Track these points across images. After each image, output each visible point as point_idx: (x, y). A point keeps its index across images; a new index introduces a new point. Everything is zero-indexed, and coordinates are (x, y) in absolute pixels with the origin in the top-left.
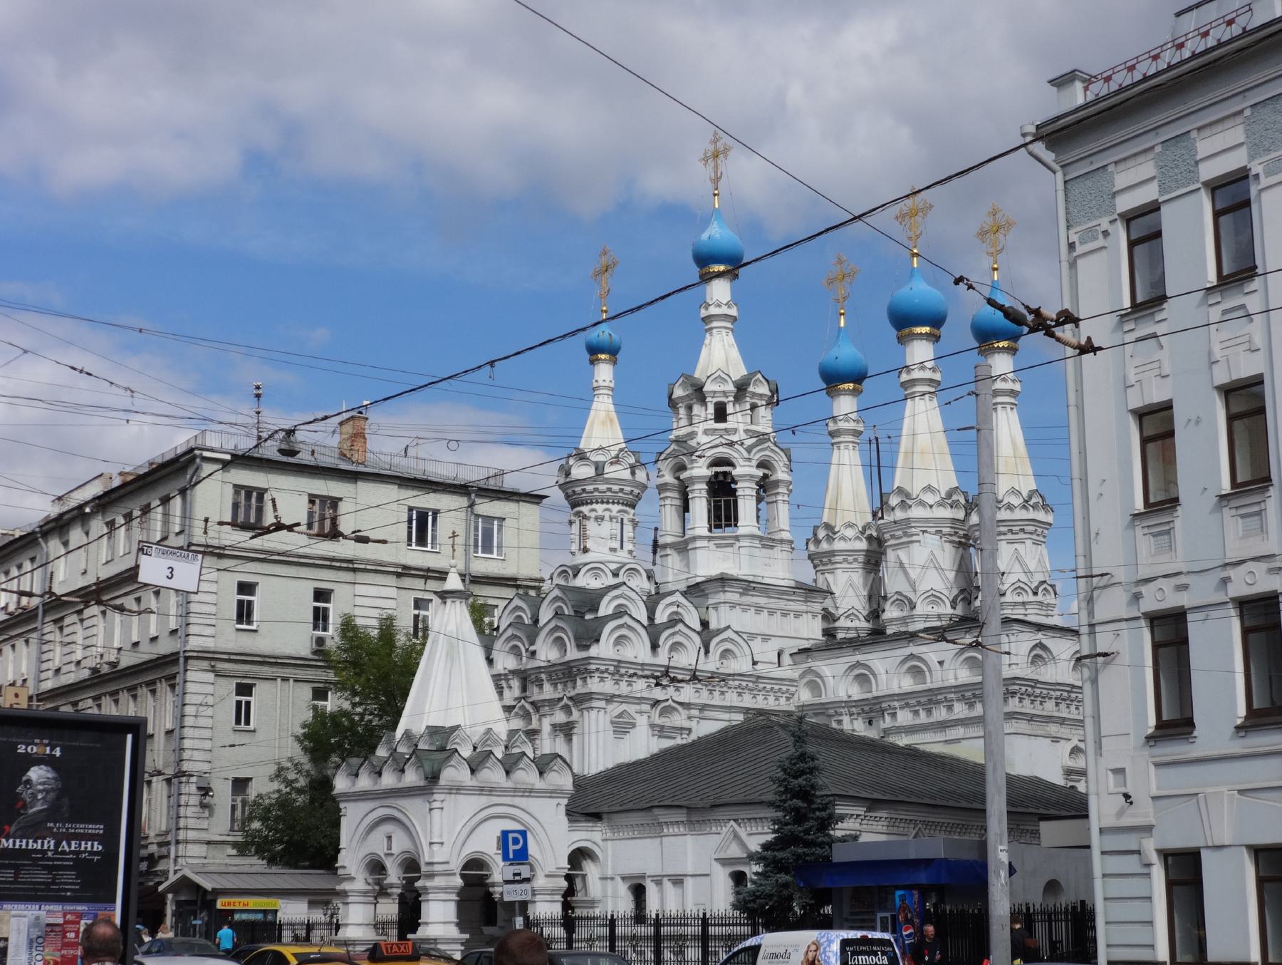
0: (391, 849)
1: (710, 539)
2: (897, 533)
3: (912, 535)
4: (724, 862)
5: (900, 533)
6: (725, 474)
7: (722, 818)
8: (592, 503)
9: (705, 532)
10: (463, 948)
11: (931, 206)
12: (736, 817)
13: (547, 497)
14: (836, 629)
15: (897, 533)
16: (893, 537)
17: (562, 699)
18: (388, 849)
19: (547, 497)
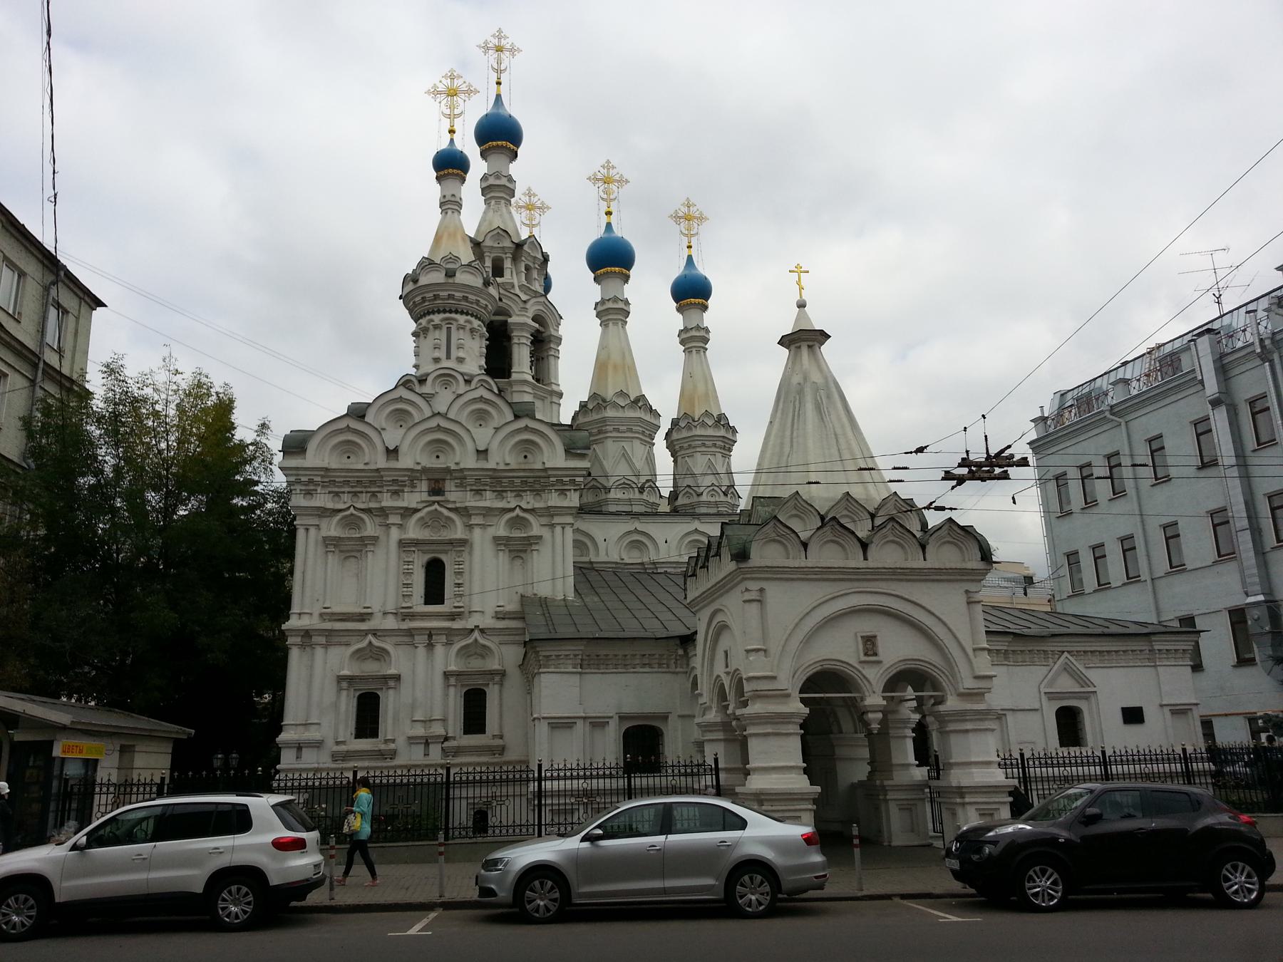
0: (875, 654)
1: (534, 387)
2: (621, 428)
3: (606, 432)
4: (1051, 696)
5: (625, 428)
6: (538, 331)
7: (1052, 649)
8: (467, 314)
9: (530, 378)
10: (1011, 799)
11: (627, 181)
12: (1069, 649)
13: (104, 305)
14: (606, 500)
15: (621, 428)
16: (618, 430)
17: (513, 510)
18: (866, 654)
19: (104, 305)
